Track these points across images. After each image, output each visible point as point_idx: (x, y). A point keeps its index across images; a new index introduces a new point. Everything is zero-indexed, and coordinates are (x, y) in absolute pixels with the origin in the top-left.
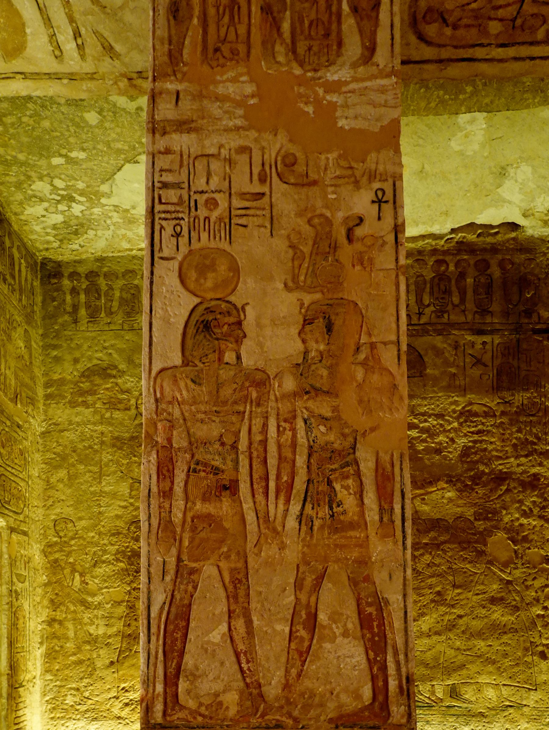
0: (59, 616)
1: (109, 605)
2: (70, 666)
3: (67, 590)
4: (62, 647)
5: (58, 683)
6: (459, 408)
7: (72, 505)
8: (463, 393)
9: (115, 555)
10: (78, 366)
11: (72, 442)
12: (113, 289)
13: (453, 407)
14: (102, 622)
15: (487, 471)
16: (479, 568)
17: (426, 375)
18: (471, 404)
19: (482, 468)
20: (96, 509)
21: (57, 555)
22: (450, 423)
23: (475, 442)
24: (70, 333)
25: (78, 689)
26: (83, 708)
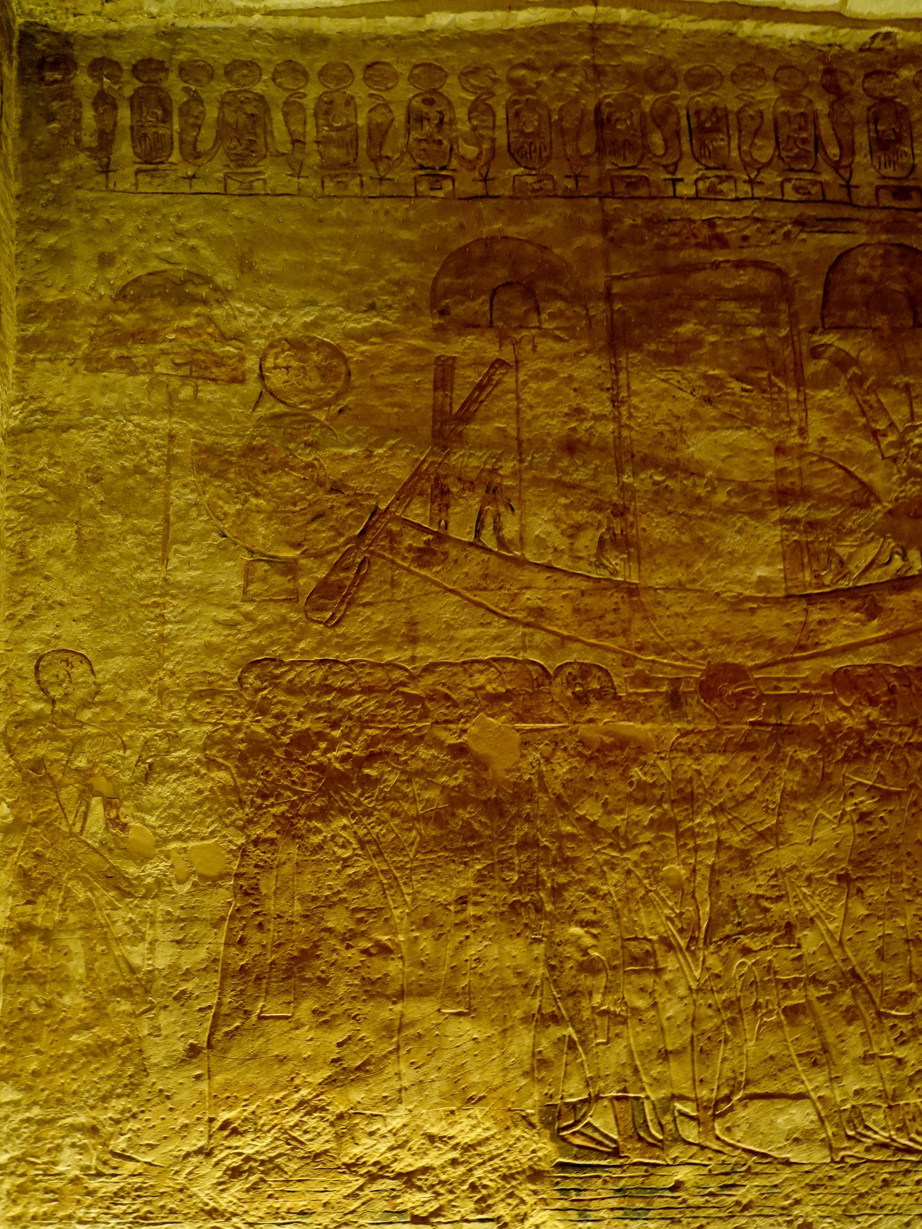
0: (43, 915)
1: (187, 887)
2: (72, 1059)
3: (68, 845)
4: (48, 1005)
5: (35, 1112)
7: (86, 617)
9: (205, 748)
10: (111, 274)
11: (90, 456)
12: (201, 102)
14: (164, 934)
20: (153, 629)
21: (41, 750)
24: (91, 195)
25: (94, 1130)
26: (109, 1186)
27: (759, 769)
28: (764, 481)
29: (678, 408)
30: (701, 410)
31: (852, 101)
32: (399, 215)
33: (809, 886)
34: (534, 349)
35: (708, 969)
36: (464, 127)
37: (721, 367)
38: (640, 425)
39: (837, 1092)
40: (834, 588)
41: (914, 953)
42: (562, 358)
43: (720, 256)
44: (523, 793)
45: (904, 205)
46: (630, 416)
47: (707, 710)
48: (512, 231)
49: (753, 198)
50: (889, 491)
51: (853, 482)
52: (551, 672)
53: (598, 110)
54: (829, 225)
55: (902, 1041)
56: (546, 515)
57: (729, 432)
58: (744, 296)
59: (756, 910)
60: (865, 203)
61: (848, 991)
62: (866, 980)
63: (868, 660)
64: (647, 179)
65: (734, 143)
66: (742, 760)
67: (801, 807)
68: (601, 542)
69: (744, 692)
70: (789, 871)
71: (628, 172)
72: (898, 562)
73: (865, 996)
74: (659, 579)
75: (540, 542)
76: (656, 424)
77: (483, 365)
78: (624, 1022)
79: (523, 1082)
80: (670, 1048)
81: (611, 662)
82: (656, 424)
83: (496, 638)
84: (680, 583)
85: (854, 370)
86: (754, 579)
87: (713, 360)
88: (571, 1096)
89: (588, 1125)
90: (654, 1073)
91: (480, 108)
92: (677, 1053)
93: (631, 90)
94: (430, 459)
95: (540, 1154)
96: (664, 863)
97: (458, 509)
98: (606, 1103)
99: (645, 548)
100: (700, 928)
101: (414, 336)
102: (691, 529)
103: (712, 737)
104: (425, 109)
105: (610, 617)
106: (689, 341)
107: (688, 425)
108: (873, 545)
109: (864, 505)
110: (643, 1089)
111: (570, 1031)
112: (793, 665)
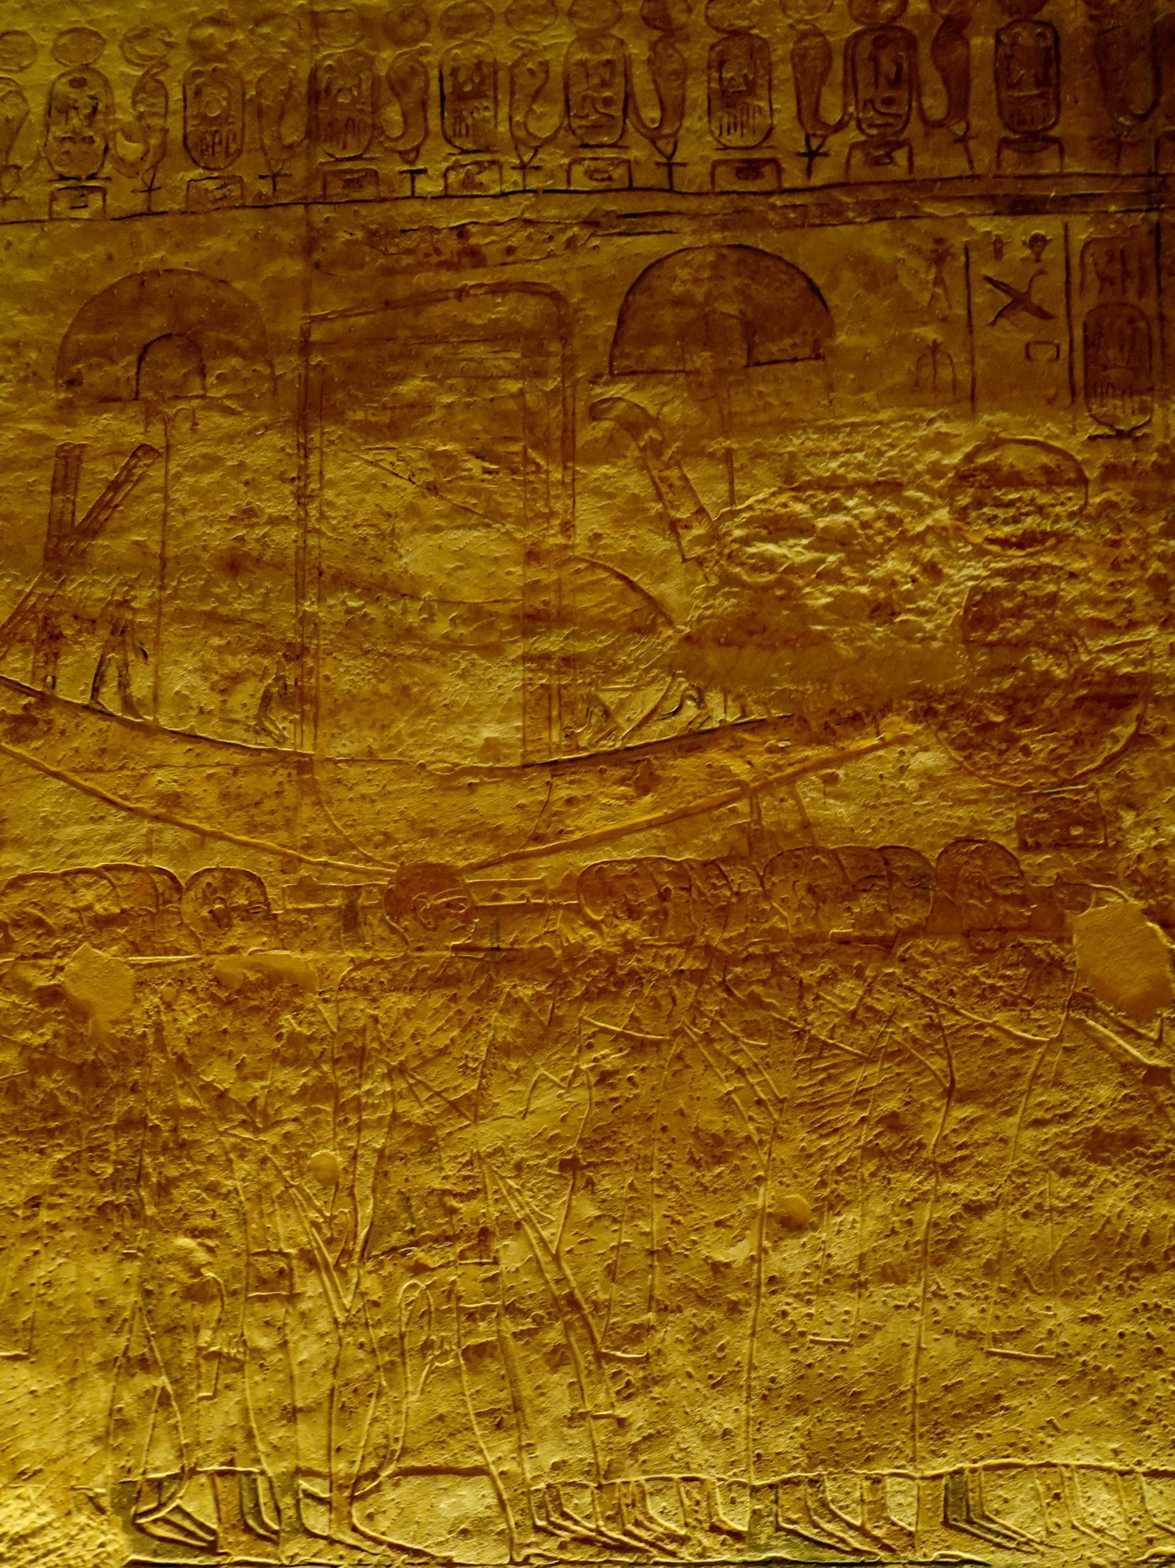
6: (955, 458)
8: (966, 406)
13: (933, 456)
15: (1059, 673)
16: (1045, 1025)
17: (833, 352)
18: (995, 443)
19: (1041, 662)
22: (922, 511)
23: (1014, 575)
27: (460, 1012)
28: (505, 601)
29: (391, 502)
30: (422, 503)
31: (687, 39)
32: (25, 247)
33: (517, 1177)
34: (193, 430)
35: (363, 1294)
36: (125, 116)
37: (453, 439)
38: (334, 529)
39: (527, 1466)
40: (593, 751)
41: (658, 1270)
42: (230, 438)
43: (470, 279)
44: (131, 1052)
45: (752, 187)
46: (322, 516)
47: (393, 930)
48: (178, 260)
49: (524, 191)
50: (688, 608)
51: (633, 597)
52: (183, 882)
53: (313, 77)
54: (632, 223)
55: (627, 1395)
56: (190, 662)
57: (460, 533)
58: (497, 336)
59: (438, 1212)
60: (694, 189)
61: (559, 1325)
62: (587, 1309)
63: (633, 854)
64: (376, 173)
65: (504, 112)
66: (436, 1000)
67: (514, 1066)
68: (266, 699)
69: (448, 905)
70: (489, 1155)
71: (347, 166)
72: (690, 710)
73: (583, 1332)
74: (343, 748)
75: (181, 700)
76: (356, 526)
77: (122, 453)
78: (240, 1369)
79: (93, 1450)
80: (299, 1404)
81: (266, 867)
82: (356, 526)
83: (110, 838)
84: (370, 752)
85: (652, 433)
86: (478, 742)
87: (446, 431)
88: (156, 1470)
89: (178, 1509)
90: (274, 1438)
91: (148, 87)
92: (308, 1411)
93: (362, 44)
94: (39, 591)
95: (109, 1549)
96: (313, 1147)
97: (70, 659)
98: (203, 1479)
99: (326, 702)
100: (355, 1236)
101: (27, 420)
102: (395, 674)
103: (397, 968)
104: (73, 94)
105: (269, 804)
106: (412, 406)
107: (402, 525)
108: (655, 687)
109: (648, 630)
110: (257, 1461)
111: (163, 1381)
112: (523, 863)
